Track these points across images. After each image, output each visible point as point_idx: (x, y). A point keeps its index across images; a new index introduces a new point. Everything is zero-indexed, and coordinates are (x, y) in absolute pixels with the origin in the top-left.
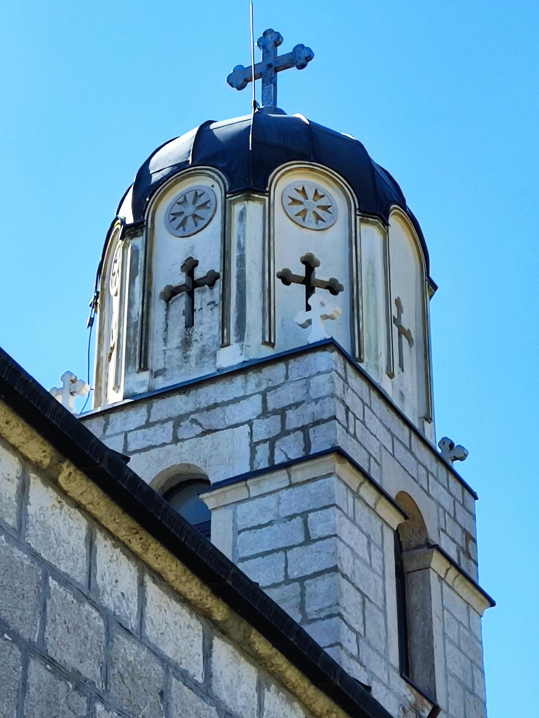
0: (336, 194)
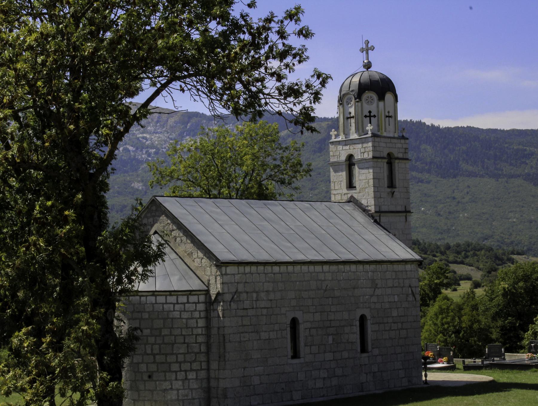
0: (374, 96)
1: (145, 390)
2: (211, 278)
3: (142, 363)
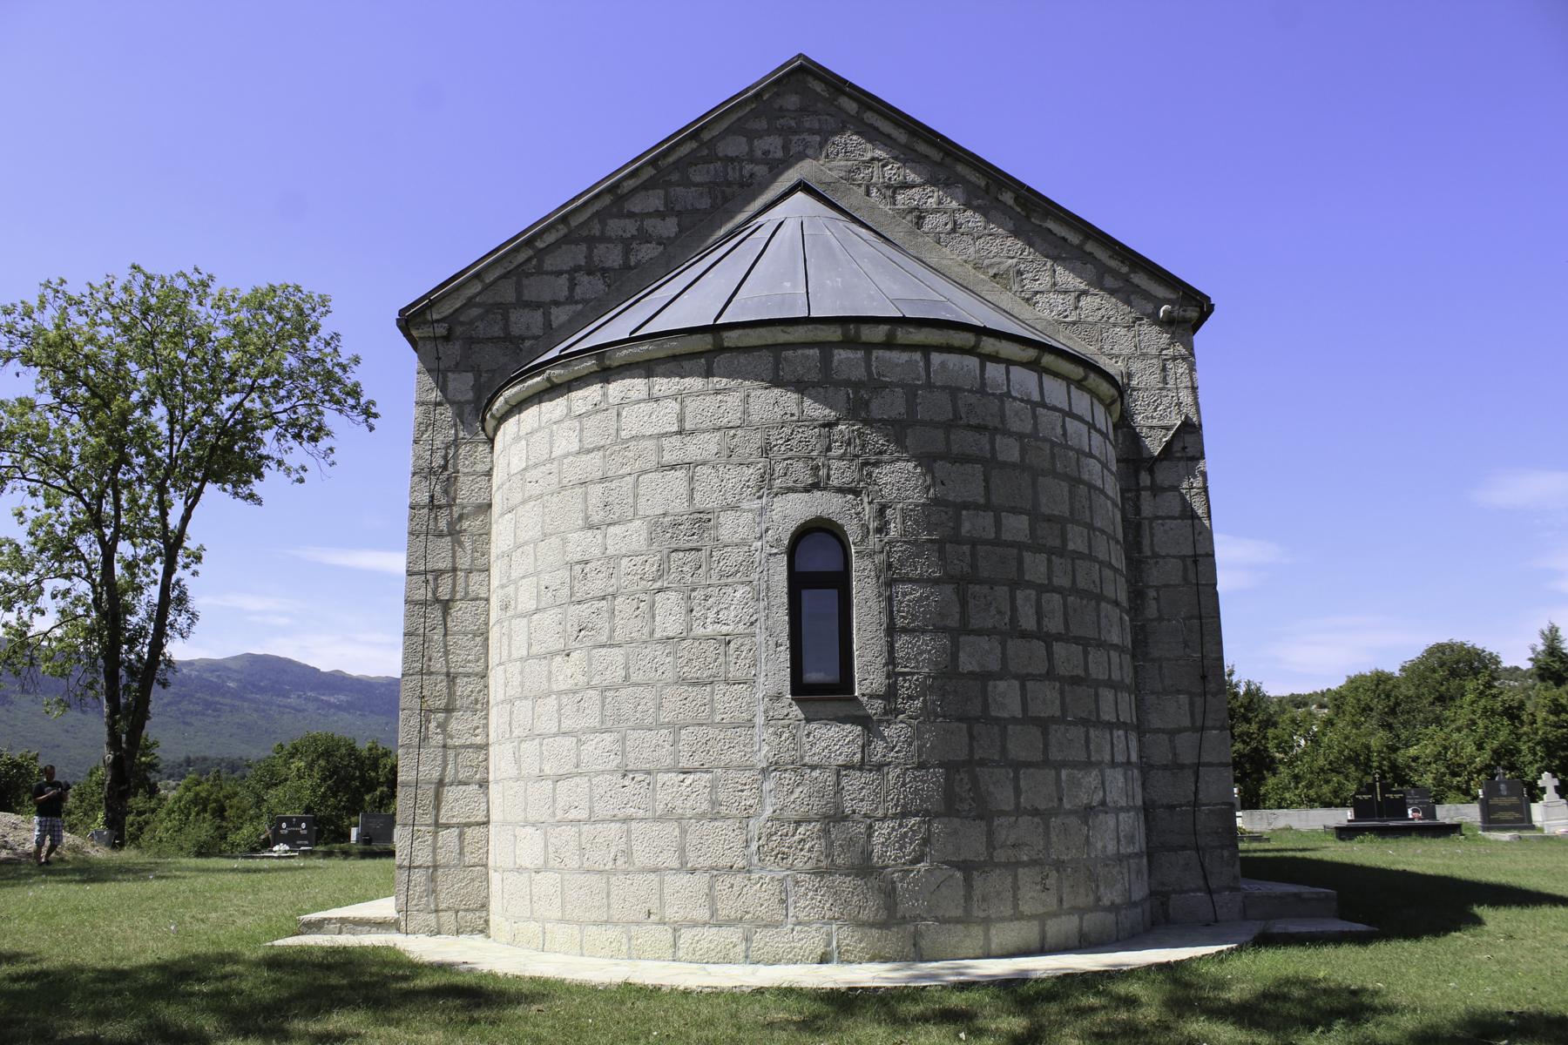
1: (1018, 811)
2: (1135, 366)
3: (1000, 676)
